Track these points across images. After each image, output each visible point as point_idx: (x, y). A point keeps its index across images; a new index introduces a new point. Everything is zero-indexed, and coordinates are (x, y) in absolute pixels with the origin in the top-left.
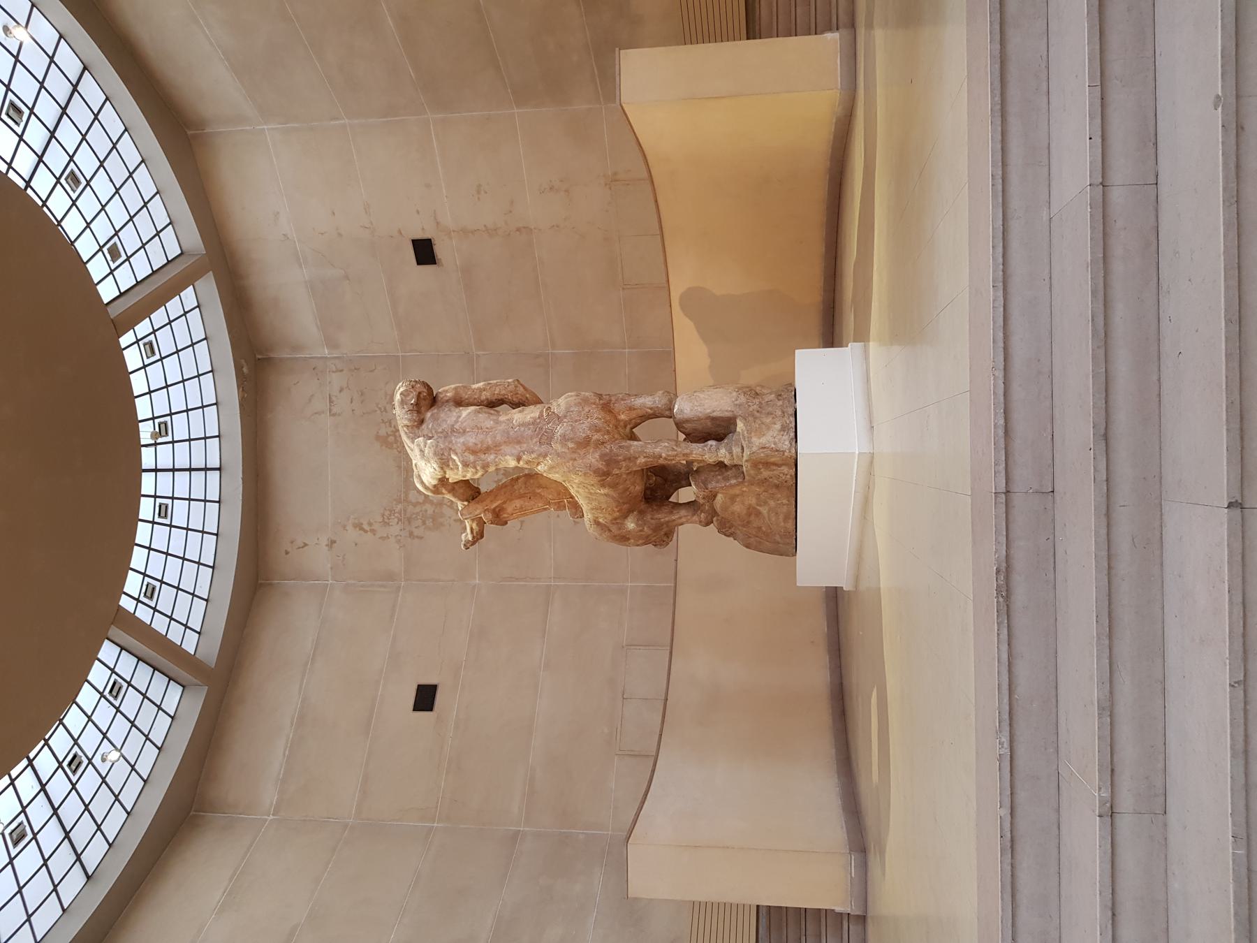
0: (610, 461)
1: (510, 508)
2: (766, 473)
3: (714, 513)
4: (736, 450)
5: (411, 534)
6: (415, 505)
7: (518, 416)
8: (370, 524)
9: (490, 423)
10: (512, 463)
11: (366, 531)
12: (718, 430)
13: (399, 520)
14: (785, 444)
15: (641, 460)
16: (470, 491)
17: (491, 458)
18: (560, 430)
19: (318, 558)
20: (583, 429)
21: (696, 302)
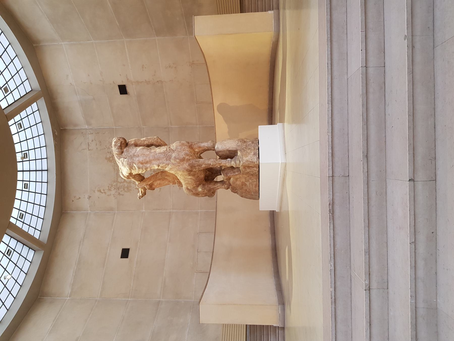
0: (192, 166)
1: (156, 184)
2: (248, 170)
3: (230, 185)
4: (238, 162)
5: (119, 193)
8: (104, 190)
10: (156, 167)
11: (102, 193)
12: (231, 155)
13: (115, 188)
14: (255, 159)
15: (204, 166)
16: (141, 178)
17: (148, 165)
18: (174, 155)
19: (85, 203)
20: (182, 155)
21: (223, 109)
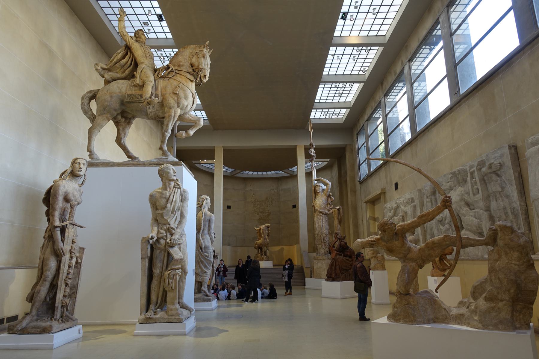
6: (257, 203)
7: (267, 236)
12: (265, 254)
16: (260, 230)
20: (265, 243)
21: (282, 250)
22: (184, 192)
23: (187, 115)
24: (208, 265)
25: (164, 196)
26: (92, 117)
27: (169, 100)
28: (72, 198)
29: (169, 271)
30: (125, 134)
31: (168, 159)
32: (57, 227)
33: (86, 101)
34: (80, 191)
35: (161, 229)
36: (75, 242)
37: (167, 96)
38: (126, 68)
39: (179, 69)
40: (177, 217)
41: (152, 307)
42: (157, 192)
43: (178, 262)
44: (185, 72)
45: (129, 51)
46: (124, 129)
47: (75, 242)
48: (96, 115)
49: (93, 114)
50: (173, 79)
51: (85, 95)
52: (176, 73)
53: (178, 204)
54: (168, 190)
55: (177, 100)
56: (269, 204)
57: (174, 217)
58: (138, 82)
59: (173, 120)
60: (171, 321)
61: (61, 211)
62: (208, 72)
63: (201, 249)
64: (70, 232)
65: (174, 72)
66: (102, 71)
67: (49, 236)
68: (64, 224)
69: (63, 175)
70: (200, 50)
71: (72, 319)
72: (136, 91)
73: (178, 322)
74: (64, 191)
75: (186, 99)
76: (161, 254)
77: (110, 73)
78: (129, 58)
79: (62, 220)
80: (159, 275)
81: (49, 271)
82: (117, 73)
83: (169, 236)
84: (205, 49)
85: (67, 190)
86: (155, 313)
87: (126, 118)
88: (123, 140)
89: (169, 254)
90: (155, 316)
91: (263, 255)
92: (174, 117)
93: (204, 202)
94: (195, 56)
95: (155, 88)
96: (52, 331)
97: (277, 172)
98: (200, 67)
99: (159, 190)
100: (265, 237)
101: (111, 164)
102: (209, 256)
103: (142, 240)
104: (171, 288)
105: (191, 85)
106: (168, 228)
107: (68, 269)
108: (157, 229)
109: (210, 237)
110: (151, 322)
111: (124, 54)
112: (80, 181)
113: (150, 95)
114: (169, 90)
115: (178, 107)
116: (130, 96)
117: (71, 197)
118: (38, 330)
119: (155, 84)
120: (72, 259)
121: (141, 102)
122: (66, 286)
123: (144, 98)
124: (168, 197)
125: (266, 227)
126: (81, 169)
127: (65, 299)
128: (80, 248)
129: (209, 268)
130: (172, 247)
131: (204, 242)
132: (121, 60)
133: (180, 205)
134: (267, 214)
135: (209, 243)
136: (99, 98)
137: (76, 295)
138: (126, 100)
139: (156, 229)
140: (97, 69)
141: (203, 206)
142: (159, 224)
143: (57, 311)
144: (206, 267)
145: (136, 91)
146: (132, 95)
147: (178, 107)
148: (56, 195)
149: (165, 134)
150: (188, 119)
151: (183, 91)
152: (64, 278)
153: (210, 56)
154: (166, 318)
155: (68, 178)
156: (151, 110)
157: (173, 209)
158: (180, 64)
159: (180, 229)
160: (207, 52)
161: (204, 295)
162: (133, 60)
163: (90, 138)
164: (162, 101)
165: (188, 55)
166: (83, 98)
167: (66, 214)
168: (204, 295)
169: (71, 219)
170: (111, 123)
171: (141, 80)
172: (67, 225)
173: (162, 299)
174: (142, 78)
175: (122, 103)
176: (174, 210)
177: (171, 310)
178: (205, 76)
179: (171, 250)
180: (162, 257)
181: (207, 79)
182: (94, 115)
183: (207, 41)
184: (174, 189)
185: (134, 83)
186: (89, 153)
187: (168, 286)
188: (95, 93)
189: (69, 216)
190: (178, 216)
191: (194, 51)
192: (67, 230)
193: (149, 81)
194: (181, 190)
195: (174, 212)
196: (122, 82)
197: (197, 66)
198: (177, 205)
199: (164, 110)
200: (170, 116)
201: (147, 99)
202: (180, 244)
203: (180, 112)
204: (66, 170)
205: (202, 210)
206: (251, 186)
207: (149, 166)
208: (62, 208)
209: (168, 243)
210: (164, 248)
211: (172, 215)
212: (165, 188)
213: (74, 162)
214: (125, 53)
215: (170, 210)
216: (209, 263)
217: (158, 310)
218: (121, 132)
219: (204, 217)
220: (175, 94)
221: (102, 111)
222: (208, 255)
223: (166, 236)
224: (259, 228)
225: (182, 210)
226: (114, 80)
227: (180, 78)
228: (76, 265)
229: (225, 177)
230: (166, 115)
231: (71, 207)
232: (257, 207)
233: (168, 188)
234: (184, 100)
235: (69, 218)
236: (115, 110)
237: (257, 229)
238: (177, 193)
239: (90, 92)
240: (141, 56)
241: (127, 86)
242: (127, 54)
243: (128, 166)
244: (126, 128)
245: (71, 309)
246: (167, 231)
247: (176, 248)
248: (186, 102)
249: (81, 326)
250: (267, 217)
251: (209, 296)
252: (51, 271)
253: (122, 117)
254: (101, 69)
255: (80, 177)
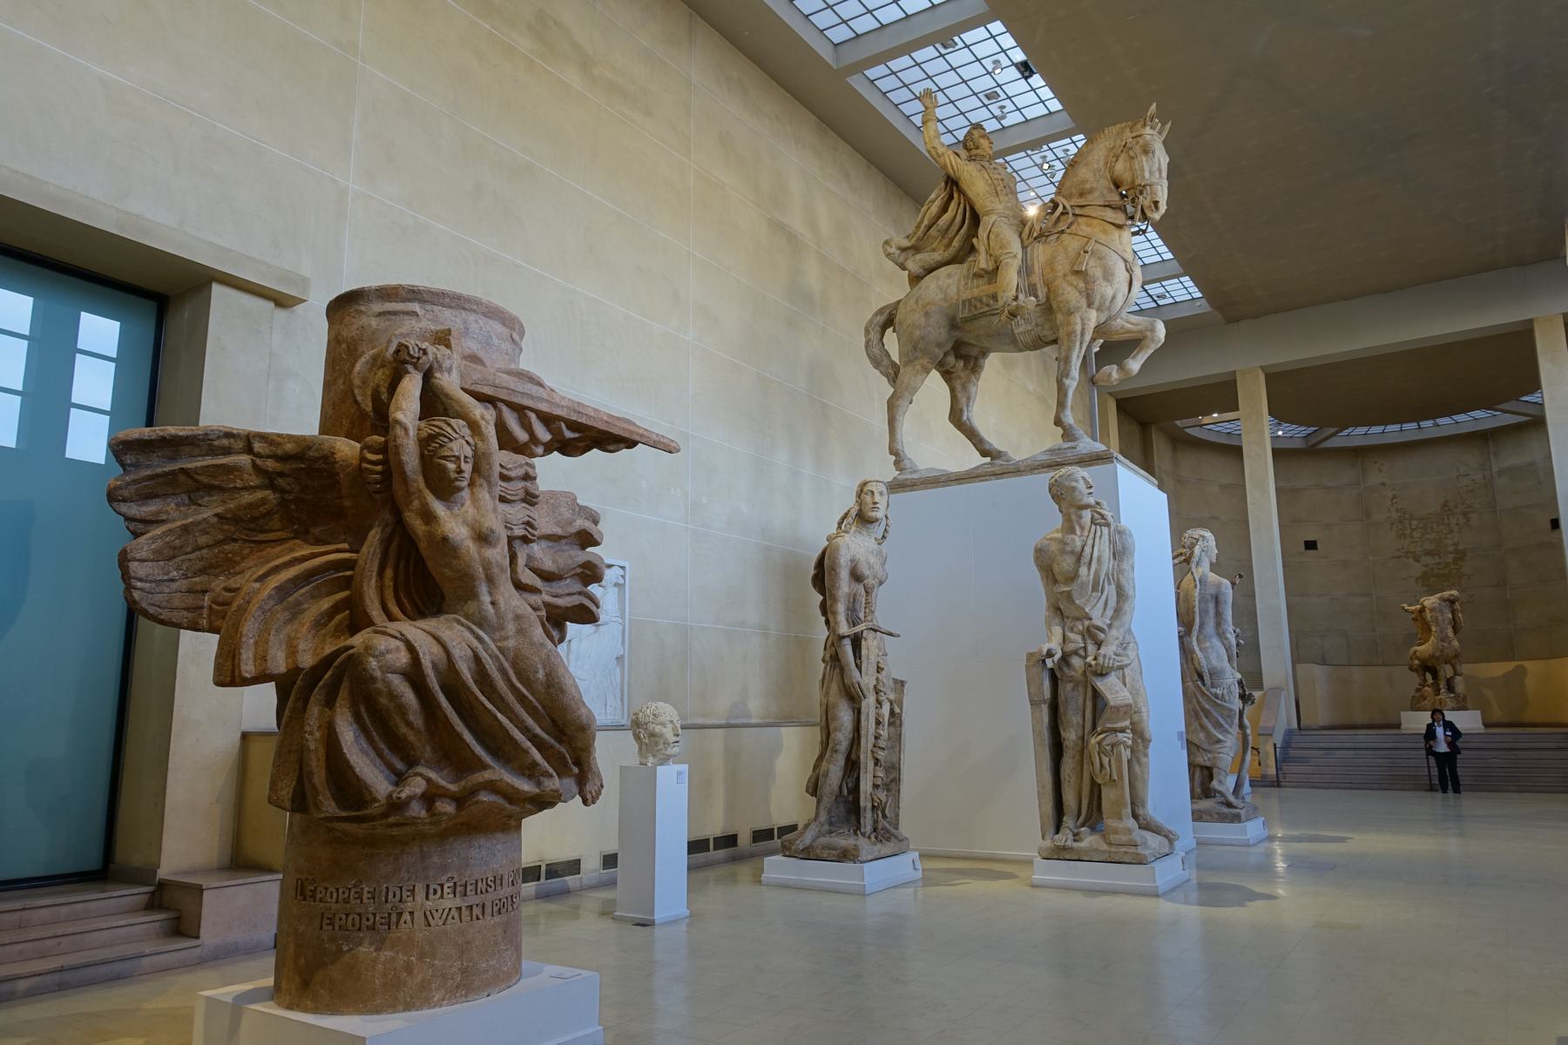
0: (1437, 659)
1: (1418, 623)
5: (1393, 524)
6: (1410, 524)
9: (1446, 622)
16: (1422, 610)
20: (1446, 651)
21: (1520, 673)
22: (1119, 532)
23: (1119, 320)
24: (1226, 722)
25: (1069, 549)
26: (891, 371)
27: (1065, 292)
28: (866, 572)
29: (1100, 734)
30: (969, 399)
31: (1078, 449)
32: (844, 637)
33: (874, 336)
34: (880, 553)
35: (1072, 630)
36: (882, 669)
37: (1060, 282)
38: (954, 233)
39: (1082, 202)
40: (1107, 598)
41: (1068, 821)
42: (1052, 539)
43: (1121, 713)
44: (1100, 206)
45: (955, 188)
46: (964, 387)
47: (882, 669)
48: (898, 363)
49: (894, 364)
50: (1070, 234)
51: (871, 322)
52: (1077, 215)
53: (1106, 565)
54: (1078, 532)
55: (1084, 289)
56: (1457, 524)
57: (1100, 598)
58: (983, 265)
59: (1081, 343)
60: (1117, 859)
61: (849, 602)
62: (1162, 191)
63: (1201, 677)
64: (870, 645)
65: (1071, 214)
66: (899, 256)
67: (831, 656)
68: (858, 629)
69: (842, 522)
70: (1134, 134)
71: (896, 837)
72: (982, 288)
73: (1134, 861)
74: (849, 557)
75: (1108, 280)
76: (1076, 693)
77: (918, 257)
78: (956, 208)
79: (853, 622)
80: (1077, 744)
81: (840, 730)
82: (934, 250)
83: (1091, 648)
84: (1148, 128)
85: (854, 556)
86: (1077, 838)
87: (966, 358)
88: (966, 413)
89: (1096, 694)
90: (1076, 845)
91: (1443, 691)
92: (1083, 334)
93: (1197, 547)
94: (1123, 156)
95: (1026, 270)
96: (860, 858)
97: (1478, 414)
98: (1138, 182)
99: (1056, 535)
100: (1441, 632)
101: (943, 479)
102: (1227, 698)
103: (1028, 660)
104: (1108, 777)
105: (1120, 236)
106: (1088, 628)
107: (876, 728)
108: (1061, 631)
109: (1224, 645)
110: (1068, 858)
111: (945, 199)
112: (878, 530)
113: (1013, 292)
114: (1062, 266)
115: (1090, 305)
116: (968, 302)
117: (864, 570)
118: (834, 852)
119: (1024, 260)
120: (881, 706)
121: (996, 312)
122: (876, 764)
123: (1001, 303)
124: (1079, 549)
125: (1443, 600)
126: (878, 506)
127: (876, 792)
128: (895, 681)
129: (1229, 729)
130: (1102, 675)
131: (1207, 658)
132: (939, 218)
133: (1113, 569)
134: (1454, 555)
135: (1222, 660)
136: (901, 324)
137: (899, 785)
138: (961, 316)
139: (1058, 630)
140: (888, 255)
141: (1195, 559)
142: (1066, 620)
143: (865, 817)
144: (1218, 725)
145: (982, 288)
146: (973, 300)
147: (1090, 305)
148: (833, 569)
149: (1064, 384)
150: (1121, 331)
151: (1098, 261)
152: (870, 746)
153: (1164, 143)
154: (1105, 852)
155: (853, 528)
156: (1021, 329)
157: (1094, 579)
158: (1083, 189)
159: (1118, 628)
160: (1154, 136)
161: (1222, 803)
162: (968, 208)
163: (892, 422)
164: (1048, 298)
165: (1102, 158)
166: (867, 331)
167: (857, 607)
168: (1222, 803)
169: (869, 618)
170: (935, 377)
171: (991, 255)
172: (862, 631)
173: (1090, 803)
174: (992, 252)
175: (953, 324)
176: (1099, 584)
177: (1116, 832)
178: (1156, 203)
179: (1100, 684)
180: (1081, 701)
181: (1163, 208)
182: (896, 364)
183: (1151, 104)
184: (1093, 527)
185: (976, 270)
186: (894, 458)
187: (1101, 771)
188: (892, 311)
189: (865, 613)
190: (1110, 597)
191: (1118, 142)
192: (863, 643)
193: (1009, 255)
194: (1112, 529)
195: (1099, 586)
196: (946, 273)
197: (1129, 180)
198: (1106, 568)
199: (1056, 320)
200: (1070, 334)
201: (1009, 305)
202: (1121, 668)
203: (1097, 317)
204: (849, 511)
205: (1194, 570)
206: (1381, 471)
207: (1032, 474)
208: (850, 594)
209: (1090, 666)
210: (1082, 678)
211: (1094, 594)
212: (1069, 528)
213: (862, 491)
214: (947, 197)
215: (1089, 581)
216: (1228, 717)
217: (1083, 829)
218: (959, 395)
219: (1200, 589)
220: (1077, 273)
221: (911, 354)
222: (1222, 695)
223: (1085, 648)
224: (1419, 607)
225: (1118, 579)
226: (930, 270)
227: (1089, 225)
228: (891, 720)
229: (1278, 454)
230: (1062, 333)
231: (867, 592)
232: (1412, 537)
233: (1077, 528)
234: (1104, 284)
235: (865, 617)
236: (939, 345)
237: (1413, 608)
238: (1101, 537)
239: (881, 311)
240: (984, 195)
241: (959, 280)
242: (951, 198)
243: (984, 478)
244: (970, 382)
245: (893, 815)
246: (1086, 636)
247: (1113, 679)
248: (1110, 288)
249: (917, 854)
250: (1452, 567)
251: (1236, 807)
252: (844, 731)
253: (958, 357)
254: (898, 252)
255: (878, 524)
